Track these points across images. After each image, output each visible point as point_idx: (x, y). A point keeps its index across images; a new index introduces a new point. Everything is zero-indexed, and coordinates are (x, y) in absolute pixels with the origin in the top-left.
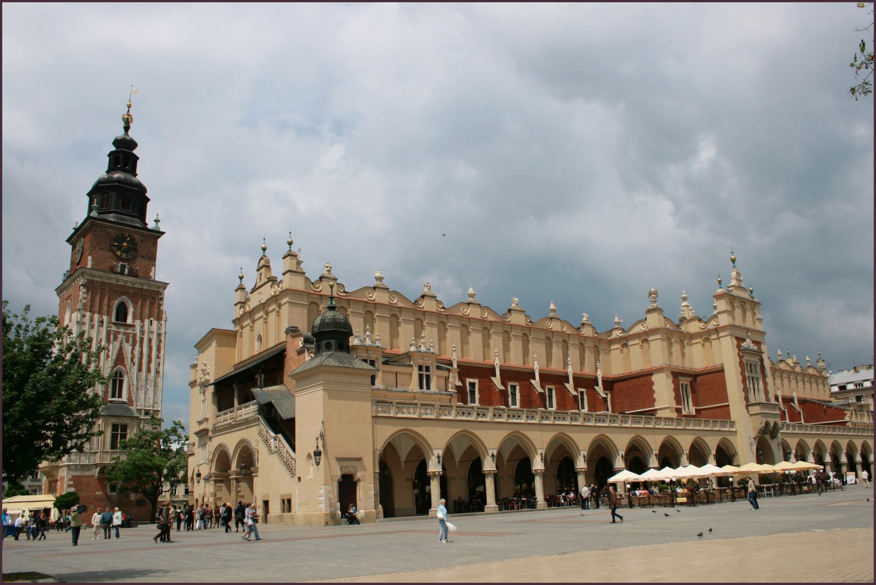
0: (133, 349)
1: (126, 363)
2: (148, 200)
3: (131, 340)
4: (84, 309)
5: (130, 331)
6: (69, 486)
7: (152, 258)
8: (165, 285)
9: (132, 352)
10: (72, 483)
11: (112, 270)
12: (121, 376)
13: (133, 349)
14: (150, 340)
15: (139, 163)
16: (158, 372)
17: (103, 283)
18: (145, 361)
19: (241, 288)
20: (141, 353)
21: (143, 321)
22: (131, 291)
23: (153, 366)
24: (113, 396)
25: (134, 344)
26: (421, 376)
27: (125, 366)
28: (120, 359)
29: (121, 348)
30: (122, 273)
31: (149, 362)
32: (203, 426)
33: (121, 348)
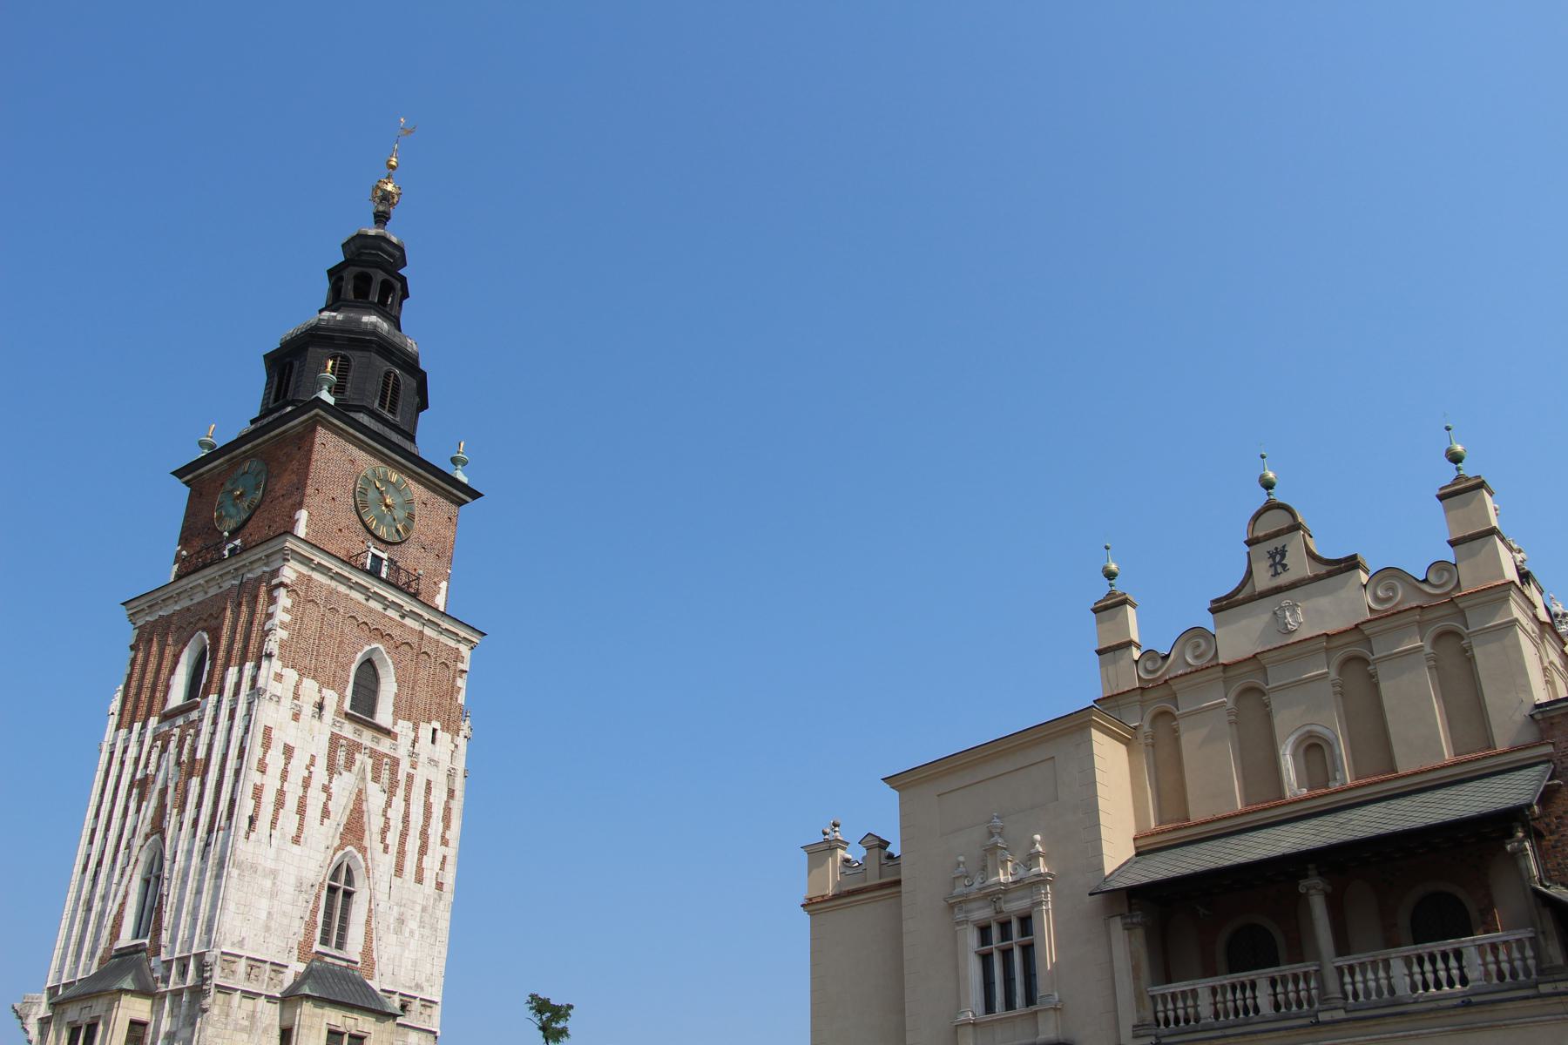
0: (389, 804)
1: (366, 843)
3: (385, 775)
13: (389, 804)
14: (429, 783)
16: (440, 886)
17: (332, 592)
18: (413, 844)
21: (416, 728)
22: (395, 632)
23: (431, 863)
24: (325, 941)
25: (391, 791)
27: (363, 850)
28: (354, 829)
30: (374, 573)
31: (423, 851)
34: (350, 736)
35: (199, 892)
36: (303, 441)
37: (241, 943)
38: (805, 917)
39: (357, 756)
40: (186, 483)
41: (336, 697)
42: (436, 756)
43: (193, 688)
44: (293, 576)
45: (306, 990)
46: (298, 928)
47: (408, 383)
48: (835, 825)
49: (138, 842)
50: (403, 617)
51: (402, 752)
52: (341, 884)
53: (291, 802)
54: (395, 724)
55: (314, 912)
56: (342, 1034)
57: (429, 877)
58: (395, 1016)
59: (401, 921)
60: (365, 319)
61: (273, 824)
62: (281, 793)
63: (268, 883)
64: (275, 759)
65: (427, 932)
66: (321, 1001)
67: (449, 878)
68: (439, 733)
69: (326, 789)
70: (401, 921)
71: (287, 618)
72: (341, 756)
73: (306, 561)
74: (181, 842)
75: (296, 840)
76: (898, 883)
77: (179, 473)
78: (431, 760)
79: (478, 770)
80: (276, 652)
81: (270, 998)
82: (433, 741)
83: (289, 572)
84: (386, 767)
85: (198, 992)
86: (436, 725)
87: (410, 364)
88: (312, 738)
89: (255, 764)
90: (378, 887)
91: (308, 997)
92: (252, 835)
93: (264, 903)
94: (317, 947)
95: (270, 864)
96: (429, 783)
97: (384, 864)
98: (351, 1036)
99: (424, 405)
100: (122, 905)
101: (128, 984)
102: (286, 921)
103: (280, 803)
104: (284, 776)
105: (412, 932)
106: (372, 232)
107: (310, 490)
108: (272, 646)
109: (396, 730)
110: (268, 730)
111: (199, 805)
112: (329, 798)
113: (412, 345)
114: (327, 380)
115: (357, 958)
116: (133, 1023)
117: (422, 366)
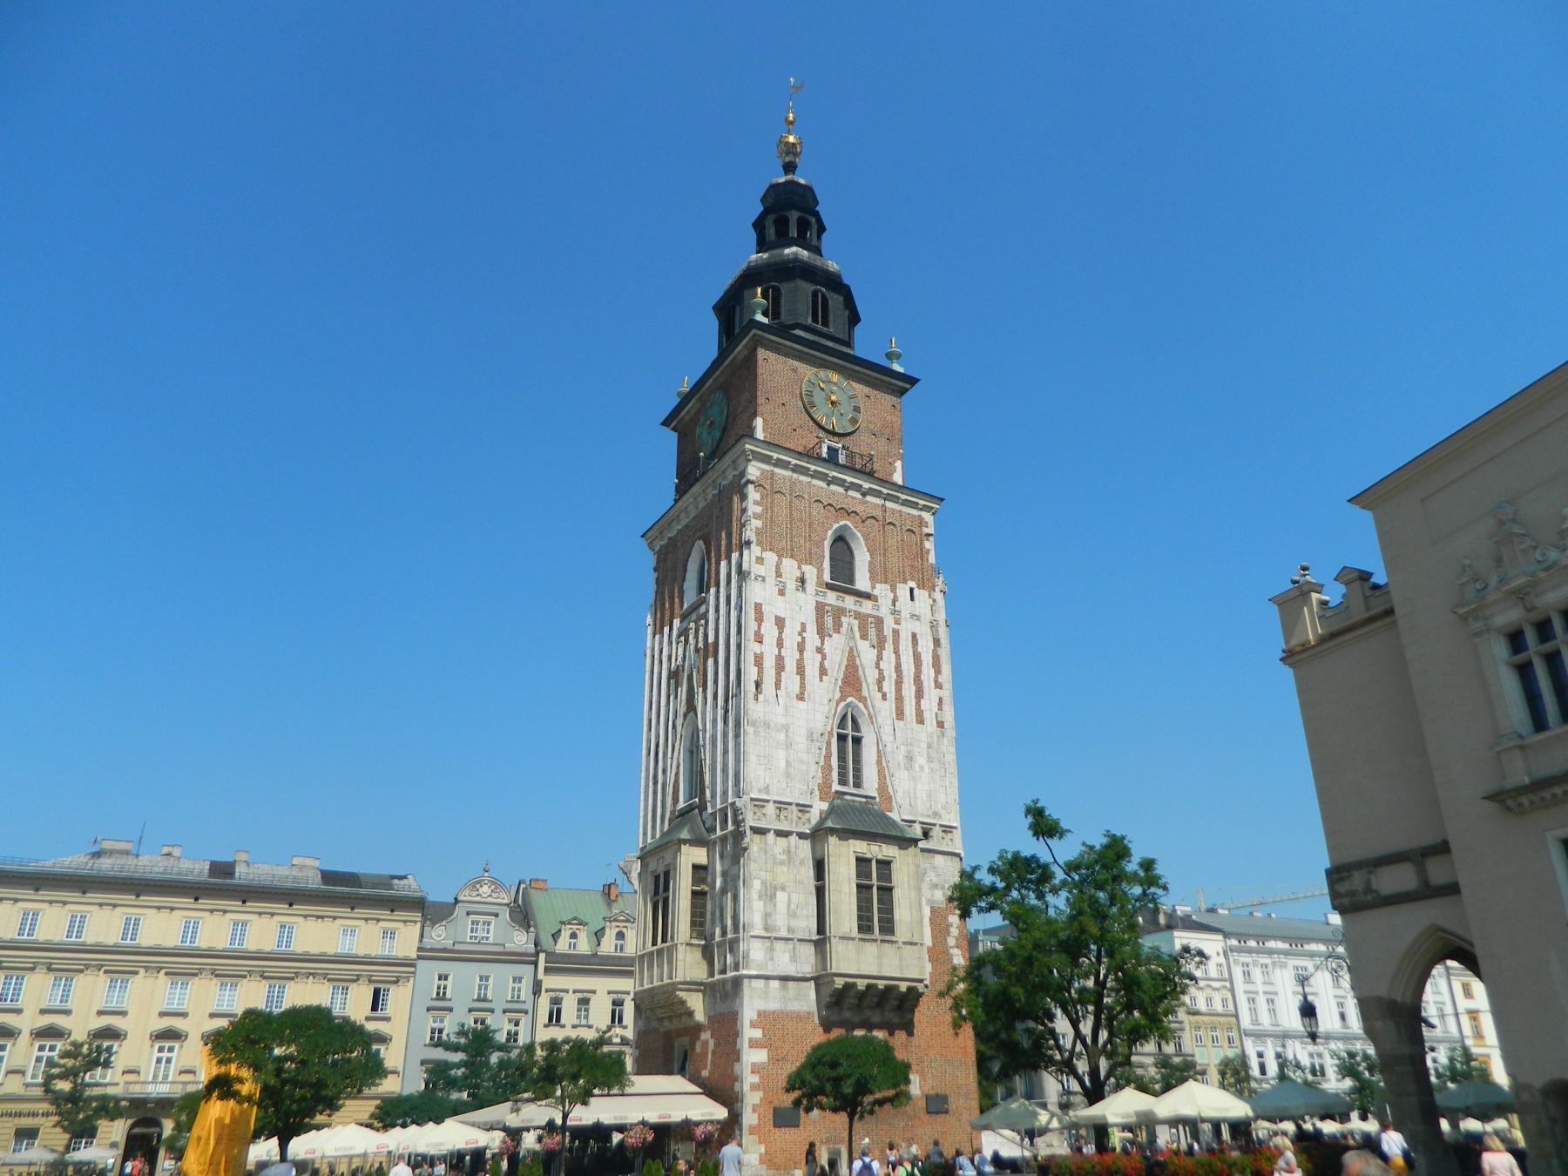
0: (880, 658)
1: (865, 693)
3: (872, 633)
4: (759, 543)
6: (754, 1044)
9: (877, 666)
12: (856, 727)
13: (880, 658)
14: (914, 636)
16: (940, 724)
18: (909, 690)
21: (893, 589)
23: (929, 704)
24: (843, 782)
25: (880, 645)
27: (863, 700)
28: (851, 681)
31: (919, 694)
34: (834, 602)
35: (725, 752)
36: (750, 363)
37: (767, 789)
38: (1288, 673)
40: (674, 429)
41: (815, 571)
42: (917, 613)
43: (702, 587)
44: (758, 473)
45: (829, 824)
46: (816, 773)
47: (835, 300)
48: (1304, 569)
49: (680, 721)
50: (864, 495)
52: (849, 731)
54: (873, 587)
55: (828, 757)
56: (869, 860)
57: (929, 717)
58: (915, 841)
59: (910, 758)
60: (787, 251)
61: (778, 685)
62: (780, 660)
63: (782, 736)
64: (770, 631)
65: (935, 766)
66: (846, 834)
67: (949, 715)
68: (916, 591)
69: (820, 650)
70: (910, 758)
71: (759, 509)
72: (829, 621)
73: (766, 459)
74: (708, 714)
75: (801, 697)
77: (665, 423)
78: (913, 616)
79: (961, 621)
80: (754, 539)
81: (801, 836)
82: (912, 599)
83: (754, 470)
84: (871, 627)
85: (738, 835)
86: (912, 584)
87: (835, 283)
88: (800, 608)
89: (752, 637)
90: (884, 732)
91: (832, 831)
92: (761, 697)
93: (781, 754)
94: (836, 787)
95: (781, 720)
96: (914, 636)
97: (886, 709)
98: (878, 862)
99: (854, 319)
100: (677, 774)
101: (685, 835)
102: (804, 767)
103: (780, 666)
104: (780, 644)
105: (922, 768)
106: (782, 180)
107: (760, 400)
108: (749, 534)
109: (876, 592)
111: (716, 681)
112: (824, 658)
113: (833, 266)
114: (759, 305)
115: (875, 794)
116: (696, 867)
117: (846, 281)
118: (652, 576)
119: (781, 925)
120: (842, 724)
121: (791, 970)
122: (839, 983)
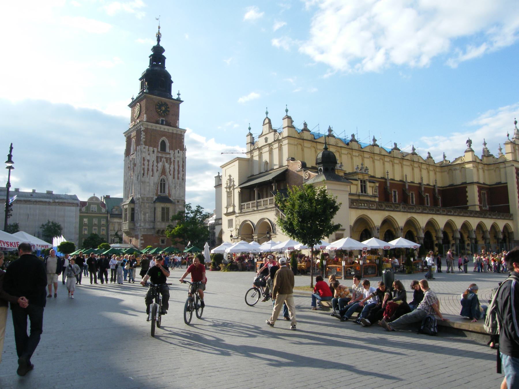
2: (172, 82)
5: (168, 156)
7: (177, 115)
8: (184, 131)
10: (142, 238)
11: (157, 122)
12: (164, 181)
15: (166, 60)
16: (183, 179)
18: (176, 173)
19: (251, 134)
20: (174, 168)
21: (174, 151)
23: (181, 176)
24: (161, 192)
26: (361, 186)
27: (166, 176)
28: (163, 172)
29: (164, 167)
31: (178, 173)
32: (231, 210)
33: (164, 167)
39: (162, 159)
51: (172, 156)
53: (150, 170)
59: (175, 187)
61: (147, 174)
69: (157, 166)
70: (175, 187)
75: (152, 176)
76: (221, 184)
84: (168, 160)
94: (159, 193)
97: (170, 178)
103: (148, 170)
104: (148, 165)
108: (142, 142)
110: (144, 158)
118: (126, 143)
119: (147, 219)
120: (161, 181)
121: (149, 227)
122: (157, 230)
